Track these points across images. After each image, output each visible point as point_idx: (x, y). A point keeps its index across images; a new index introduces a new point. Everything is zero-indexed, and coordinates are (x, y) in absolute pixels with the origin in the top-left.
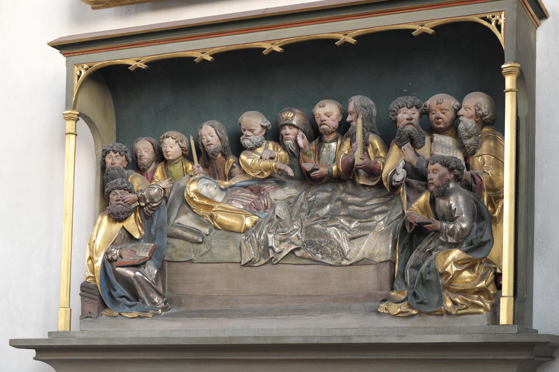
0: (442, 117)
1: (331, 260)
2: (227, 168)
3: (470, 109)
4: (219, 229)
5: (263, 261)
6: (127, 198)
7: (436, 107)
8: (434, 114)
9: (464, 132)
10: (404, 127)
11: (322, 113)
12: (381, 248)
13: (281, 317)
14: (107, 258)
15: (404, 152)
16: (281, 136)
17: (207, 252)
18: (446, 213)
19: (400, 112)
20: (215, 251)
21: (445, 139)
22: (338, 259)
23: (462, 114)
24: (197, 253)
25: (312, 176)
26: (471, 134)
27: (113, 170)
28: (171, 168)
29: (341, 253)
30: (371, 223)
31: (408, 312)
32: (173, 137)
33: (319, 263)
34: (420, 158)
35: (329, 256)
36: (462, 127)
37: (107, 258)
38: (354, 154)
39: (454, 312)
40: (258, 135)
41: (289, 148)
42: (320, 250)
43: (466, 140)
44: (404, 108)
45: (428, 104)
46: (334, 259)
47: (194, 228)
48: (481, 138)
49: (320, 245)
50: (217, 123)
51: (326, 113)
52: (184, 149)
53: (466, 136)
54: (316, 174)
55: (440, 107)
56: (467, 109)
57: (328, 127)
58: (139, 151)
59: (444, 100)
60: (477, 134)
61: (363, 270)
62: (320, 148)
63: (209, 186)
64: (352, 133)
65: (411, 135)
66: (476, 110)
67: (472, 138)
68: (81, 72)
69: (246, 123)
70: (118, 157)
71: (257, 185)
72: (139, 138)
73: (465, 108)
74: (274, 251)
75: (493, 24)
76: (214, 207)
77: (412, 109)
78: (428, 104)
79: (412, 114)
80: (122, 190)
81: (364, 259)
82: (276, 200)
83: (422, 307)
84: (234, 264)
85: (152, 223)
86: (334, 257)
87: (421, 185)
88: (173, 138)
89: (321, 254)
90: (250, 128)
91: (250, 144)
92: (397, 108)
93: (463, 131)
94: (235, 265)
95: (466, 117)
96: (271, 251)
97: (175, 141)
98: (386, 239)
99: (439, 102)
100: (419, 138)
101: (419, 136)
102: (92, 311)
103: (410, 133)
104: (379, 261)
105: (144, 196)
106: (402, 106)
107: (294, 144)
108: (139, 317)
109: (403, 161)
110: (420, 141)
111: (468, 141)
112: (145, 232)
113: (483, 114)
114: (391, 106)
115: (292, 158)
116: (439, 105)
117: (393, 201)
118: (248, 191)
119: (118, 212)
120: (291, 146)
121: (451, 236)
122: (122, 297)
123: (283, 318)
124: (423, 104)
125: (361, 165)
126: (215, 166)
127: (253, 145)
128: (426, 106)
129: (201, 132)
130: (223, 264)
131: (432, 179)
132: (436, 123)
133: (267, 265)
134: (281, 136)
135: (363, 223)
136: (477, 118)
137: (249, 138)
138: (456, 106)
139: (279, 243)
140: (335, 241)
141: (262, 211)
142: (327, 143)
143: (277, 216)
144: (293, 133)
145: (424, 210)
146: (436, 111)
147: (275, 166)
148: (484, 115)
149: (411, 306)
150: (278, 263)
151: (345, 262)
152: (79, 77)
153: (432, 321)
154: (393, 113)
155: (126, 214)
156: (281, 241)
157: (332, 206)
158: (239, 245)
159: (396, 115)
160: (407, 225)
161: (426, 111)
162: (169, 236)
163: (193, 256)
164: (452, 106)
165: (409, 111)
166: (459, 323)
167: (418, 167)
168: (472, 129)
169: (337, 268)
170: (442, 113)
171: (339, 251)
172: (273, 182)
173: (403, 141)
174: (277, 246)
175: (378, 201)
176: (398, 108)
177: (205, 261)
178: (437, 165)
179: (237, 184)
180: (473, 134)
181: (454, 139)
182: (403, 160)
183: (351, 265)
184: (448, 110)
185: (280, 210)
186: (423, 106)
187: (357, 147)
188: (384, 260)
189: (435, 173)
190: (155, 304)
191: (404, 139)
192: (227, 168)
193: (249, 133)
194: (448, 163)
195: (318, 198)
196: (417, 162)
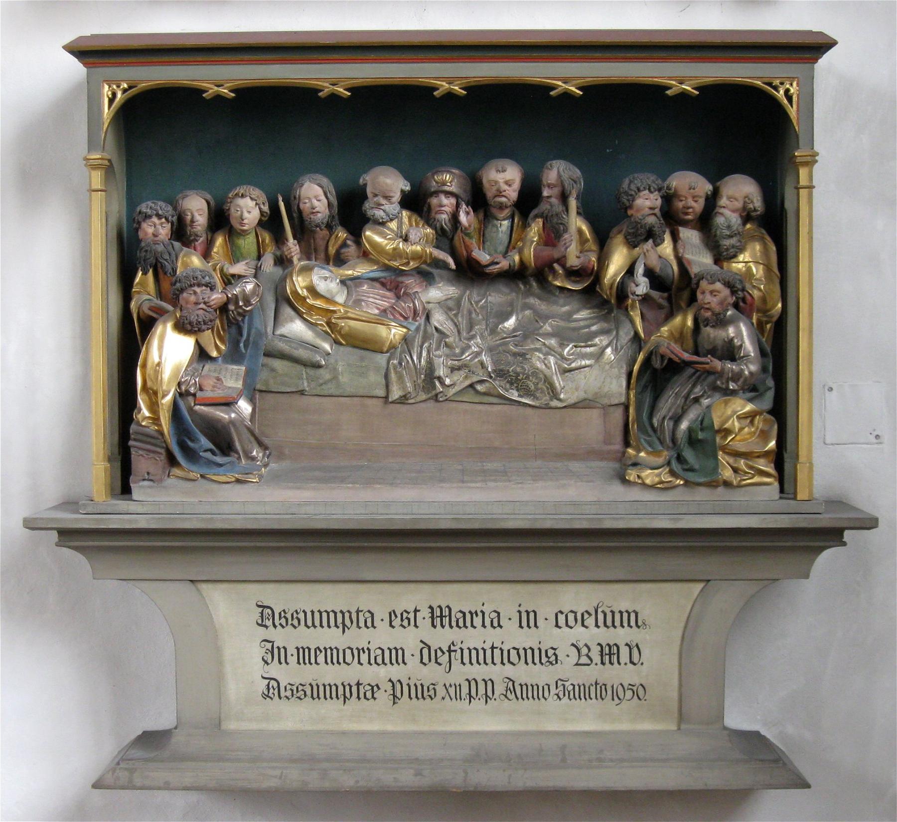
1: (533, 399)
2: (333, 245)
4: (341, 344)
5: (423, 396)
6: (213, 300)
8: (681, 201)
11: (501, 181)
12: (611, 386)
13: (473, 485)
14: (178, 390)
16: (427, 206)
17: (330, 381)
18: (719, 348)
19: (640, 197)
20: (344, 379)
21: (692, 235)
22: (544, 398)
23: (724, 205)
24: (312, 381)
27: (157, 246)
28: (241, 242)
29: (550, 390)
30: (591, 348)
31: (670, 481)
32: (253, 196)
33: (513, 403)
35: (528, 393)
37: (178, 390)
38: (567, 248)
39: (735, 483)
41: (442, 225)
42: (515, 385)
44: (644, 192)
45: (674, 186)
46: (537, 399)
47: (308, 344)
49: (517, 377)
50: (325, 181)
52: (265, 214)
53: (726, 235)
54: (495, 269)
58: (189, 214)
61: (582, 415)
62: (485, 227)
63: (329, 280)
64: (550, 214)
66: (745, 202)
67: (734, 238)
68: (114, 95)
70: (164, 225)
71: (393, 277)
72: (189, 192)
73: (729, 198)
74: (442, 383)
75: (782, 92)
76: (338, 312)
78: (674, 186)
80: (204, 288)
81: (585, 400)
82: (429, 303)
83: (691, 476)
84: (374, 399)
85: (240, 334)
86: (538, 395)
87: (663, 298)
88: (252, 199)
89: (518, 390)
90: (388, 195)
91: (384, 217)
92: (635, 192)
94: (374, 401)
96: (437, 384)
97: (254, 202)
98: (618, 373)
101: (660, 229)
102: (151, 470)
103: (651, 227)
104: (609, 404)
105: (236, 296)
107: (449, 220)
108: (238, 481)
110: (660, 237)
112: (226, 347)
114: (624, 186)
115: (440, 238)
116: (692, 191)
117: (613, 315)
118: (377, 285)
119: (199, 322)
121: (734, 381)
122: (206, 451)
123: (478, 488)
125: (577, 266)
126: (312, 241)
127: (388, 218)
128: (669, 188)
129: (299, 192)
130: (355, 399)
131: (710, 303)
133: (429, 401)
134: (427, 206)
135: (579, 349)
137: (382, 207)
139: (449, 372)
140: (541, 373)
141: (410, 320)
142: (499, 220)
143: (436, 329)
144: (450, 203)
145: (679, 337)
146: (686, 198)
147: (431, 254)
148: (755, 210)
149: (672, 473)
150: (446, 400)
151: (555, 403)
152: (111, 101)
153: (702, 494)
154: (629, 197)
155: (210, 323)
156: (453, 369)
157: (520, 317)
158: (383, 372)
159: (633, 201)
160: (656, 357)
162: (268, 354)
163: (306, 384)
165: (652, 196)
166: (738, 497)
167: (662, 274)
168: (736, 226)
169: (541, 410)
171: (546, 386)
174: (447, 376)
175: (590, 314)
177: (326, 393)
178: (718, 286)
183: (565, 407)
184: (701, 197)
185: (439, 319)
187: (572, 240)
188: (616, 402)
189: (715, 296)
190: (253, 459)
192: (333, 245)
193: (383, 201)
195: (490, 302)
196: (660, 268)
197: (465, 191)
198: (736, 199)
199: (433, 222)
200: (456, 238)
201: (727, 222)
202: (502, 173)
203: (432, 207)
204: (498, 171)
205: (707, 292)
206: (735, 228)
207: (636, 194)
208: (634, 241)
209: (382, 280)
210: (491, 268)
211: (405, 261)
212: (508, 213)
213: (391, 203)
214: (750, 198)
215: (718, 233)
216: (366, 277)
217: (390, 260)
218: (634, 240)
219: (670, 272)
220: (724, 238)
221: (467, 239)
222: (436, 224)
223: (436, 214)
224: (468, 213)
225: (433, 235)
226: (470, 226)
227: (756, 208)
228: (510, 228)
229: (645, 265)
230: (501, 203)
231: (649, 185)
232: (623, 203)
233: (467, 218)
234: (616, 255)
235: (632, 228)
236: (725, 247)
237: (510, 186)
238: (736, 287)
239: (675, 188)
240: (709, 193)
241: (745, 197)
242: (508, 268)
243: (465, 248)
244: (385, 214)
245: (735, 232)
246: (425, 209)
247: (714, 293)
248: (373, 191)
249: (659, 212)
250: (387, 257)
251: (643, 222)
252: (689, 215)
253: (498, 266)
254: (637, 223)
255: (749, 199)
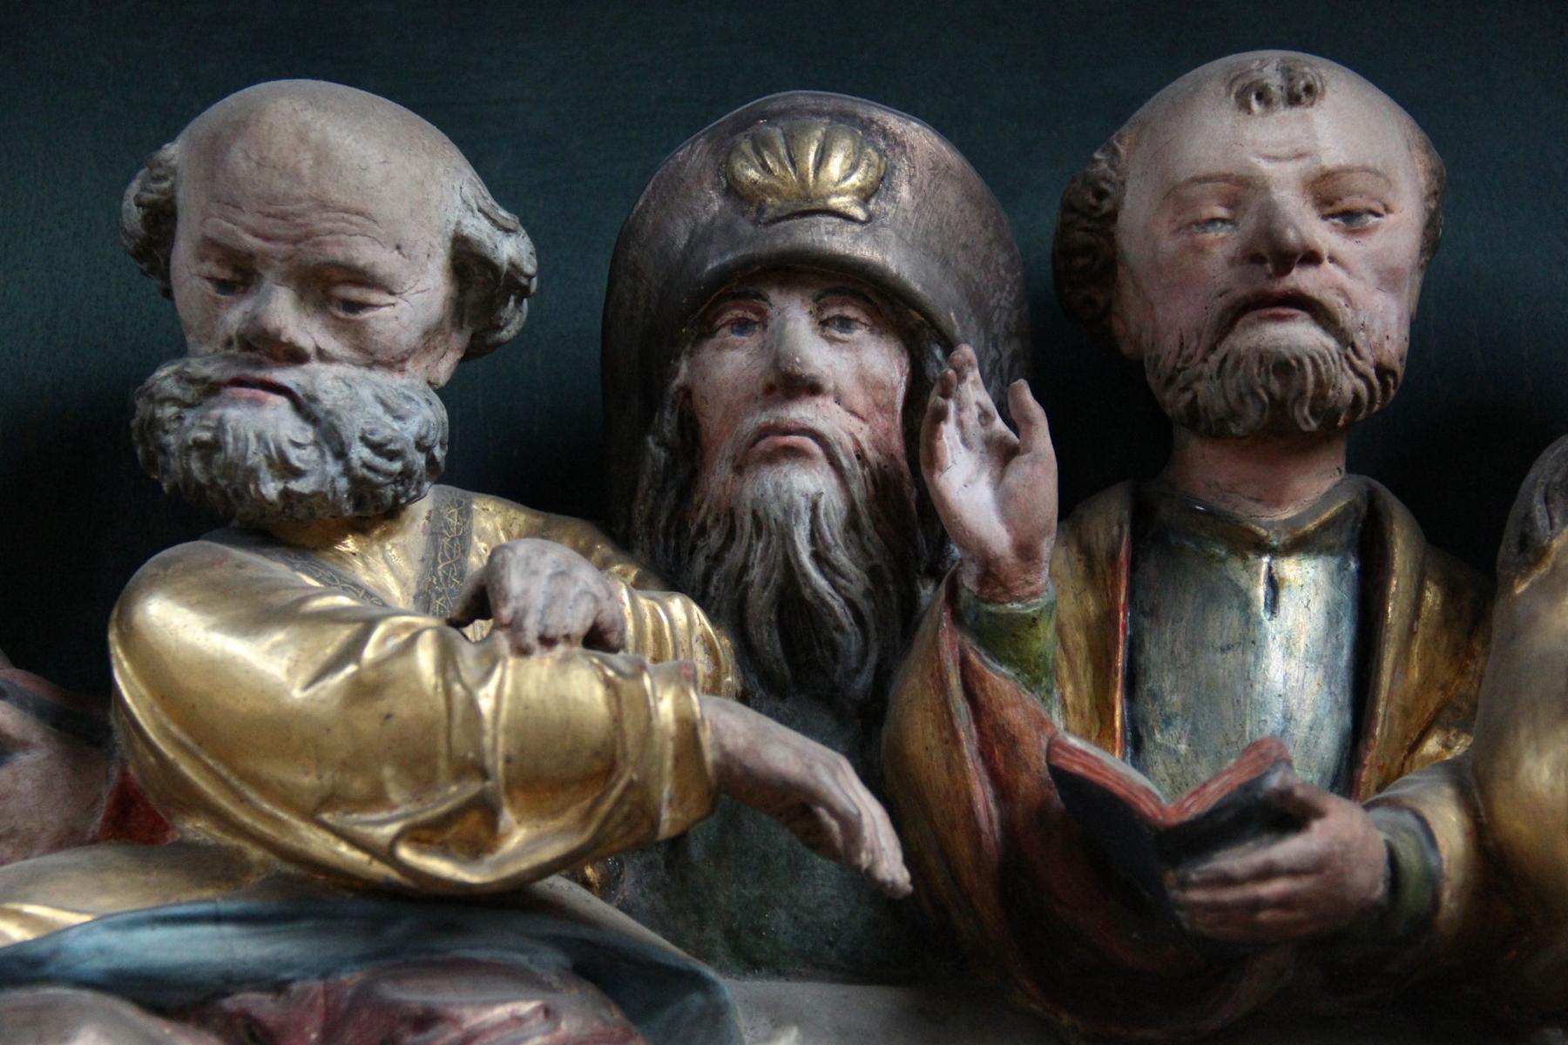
16: (668, 422)
25: (1198, 896)
40: (394, 363)
51: (1327, 176)
54: (1268, 873)
57: (1331, 343)
69: (297, 176)
71: (351, 978)
90: (338, 254)
91: (294, 456)
107: (852, 523)
120: (815, 535)
127: (333, 468)
134: (668, 422)
137: (287, 376)
142: (1261, 547)
144: (863, 379)
147: (689, 730)
172: (551, 959)
179: (82, 944)
197: (976, 302)
199: (716, 559)
200: (911, 688)
202: (1283, 112)
203: (712, 418)
204: (1253, 95)
209: (261, 1005)
210: (1235, 860)
211: (455, 793)
212: (1328, 497)
213: (375, 358)
216: (99, 964)
217: (330, 800)
221: (1000, 679)
222: (745, 568)
223: (739, 469)
224: (1004, 454)
225: (716, 662)
226: (1026, 551)
228: (1346, 630)
230: (1284, 366)
233: (998, 482)
237: (1350, 219)
242: (1380, 890)
243: (985, 754)
244: (307, 434)
246: (656, 452)
248: (218, 226)
250: (307, 780)
253: (1290, 849)
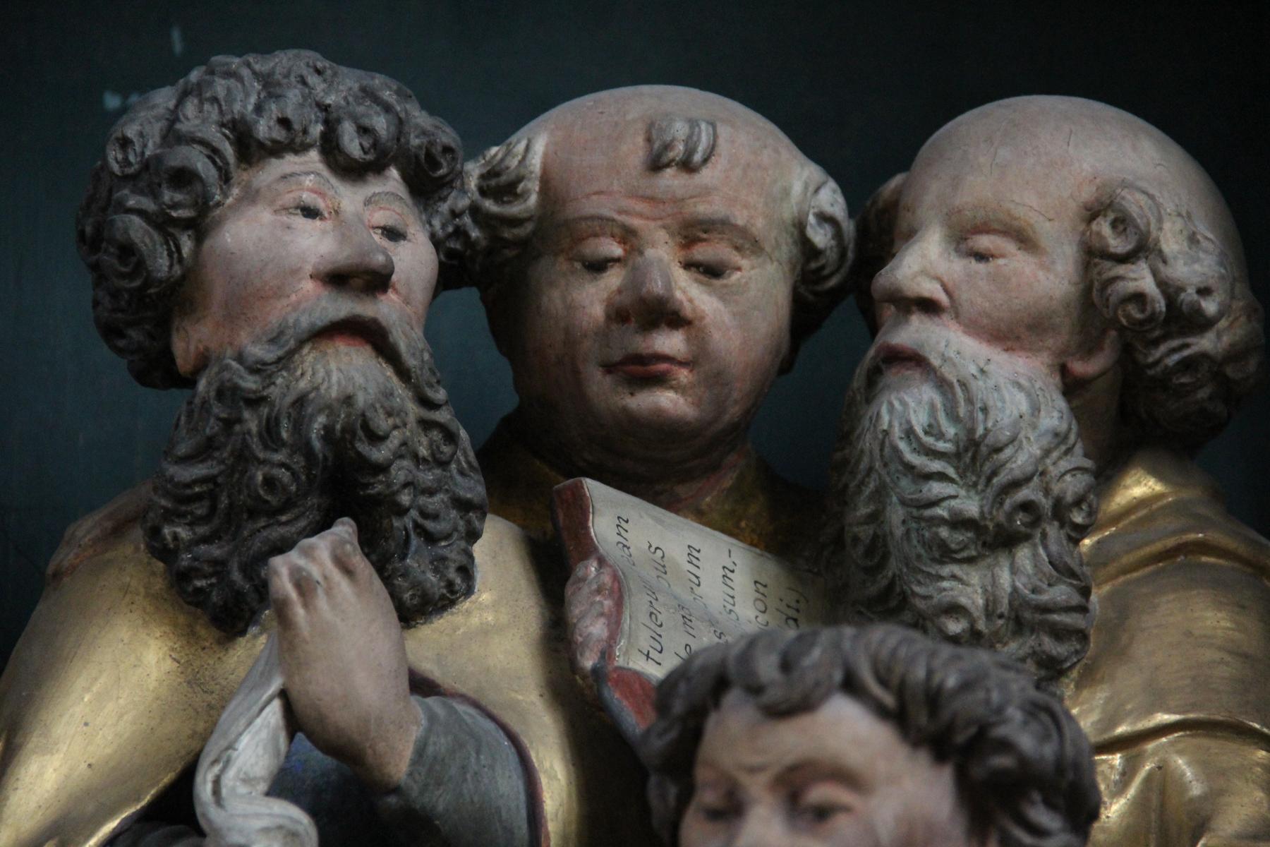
0: (688, 311)
3: (1024, 240)
7: (634, 195)
8: (598, 266)
9: (942, 477)
10: (291, 353)
15: (299, 612)
19: (251, 196)
26: (1027, 506)
34: (453, 711)
36: (919, 421)
43: (956, 569)
44: (290, 163)
48: (1101, 556)
53: (959, 522)
55: (678, 201)
56: (984, 242)
59: (724, 132)
60: (1078, 518)
65: (363, 447)
66: (1092, 254)
67: (1023, 554)
77: (374, 187)
78: (536, 162)
79: (377, 237)
92: (214, 153)
93: (936, 466)
95: (976, 328)
99: (679, 150)
100: (435, 502)
101: (428, 477)
103: (349, 430)
106: (279, 134)
109: (275, 709)
110: (431, 538)
111: (975, 576)
113: (1171, 300)
114: (131, 131)
116: (671, 179)
124: (473, 171)
132: (609, 368)
136: (1088, 348)
138: (824, 218)
146: (628, 236)
154: (168, 195)
161: (497, 243)
164: (788, 211)
165: (350, 197)
167: (440, 801)
170: (688, 265)
173: (253, 514)
176: (228, 150)
180: (1046, 504)
181: (771, 569)
182: (276, 705)
186: (473, 183)
189: (823, 813)
191: (270, 482)
194: (971, 704)
196: (420, 751)
198: (1024, 240)
201: (954, 417)
205: (757, 789)
206: (1020, 460)
207: (226, 178)
208: (219, 566)
214: (1134, 211)
215: (896, 515)
218: (216, 551)
219: (508, 785)
220: (946, 554)
227: (1190, 295)
229: (294, 721)
231: (325, 108)
232: (127, 250)
234: (81, 682)
235: (205, 450)
236: (955, 626)
238: (1005, 746)
239: (545, 180)
240: (820, 237)
241: (1092, 213)
245: (1024, 494)
247: (820, 793)
249: (418, 333)
251: (281, 390)
252: (659, 381)
254: (229, 393)
255: (1122, 223)
